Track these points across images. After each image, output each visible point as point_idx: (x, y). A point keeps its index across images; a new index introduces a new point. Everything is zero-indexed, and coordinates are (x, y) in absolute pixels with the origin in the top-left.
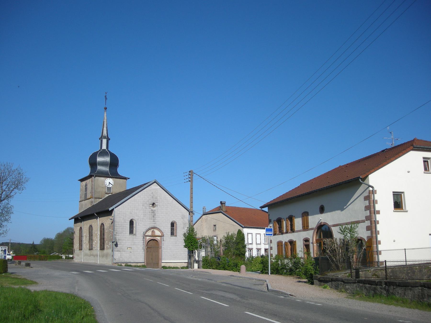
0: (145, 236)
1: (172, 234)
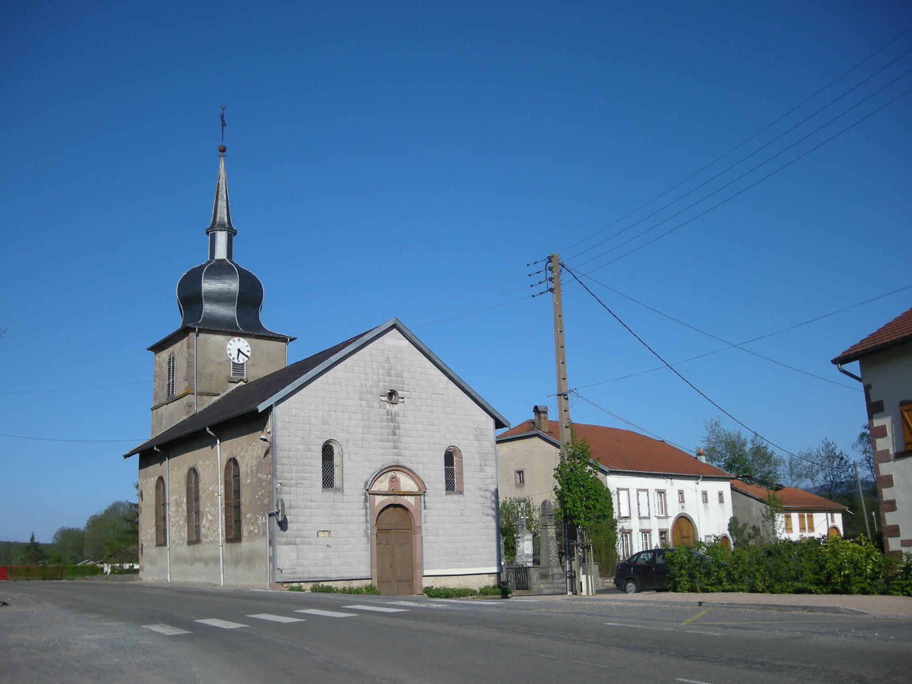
0: (369, 493)
1: (450, 486)
